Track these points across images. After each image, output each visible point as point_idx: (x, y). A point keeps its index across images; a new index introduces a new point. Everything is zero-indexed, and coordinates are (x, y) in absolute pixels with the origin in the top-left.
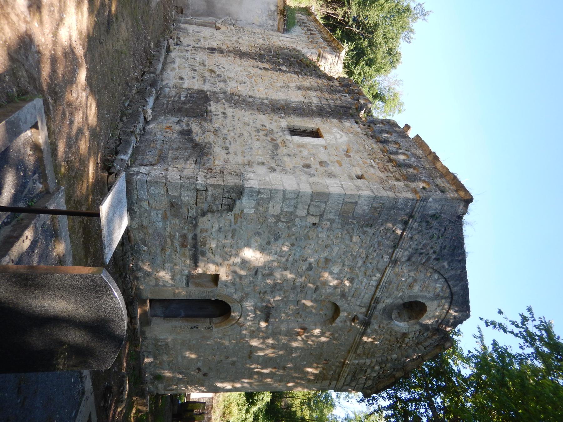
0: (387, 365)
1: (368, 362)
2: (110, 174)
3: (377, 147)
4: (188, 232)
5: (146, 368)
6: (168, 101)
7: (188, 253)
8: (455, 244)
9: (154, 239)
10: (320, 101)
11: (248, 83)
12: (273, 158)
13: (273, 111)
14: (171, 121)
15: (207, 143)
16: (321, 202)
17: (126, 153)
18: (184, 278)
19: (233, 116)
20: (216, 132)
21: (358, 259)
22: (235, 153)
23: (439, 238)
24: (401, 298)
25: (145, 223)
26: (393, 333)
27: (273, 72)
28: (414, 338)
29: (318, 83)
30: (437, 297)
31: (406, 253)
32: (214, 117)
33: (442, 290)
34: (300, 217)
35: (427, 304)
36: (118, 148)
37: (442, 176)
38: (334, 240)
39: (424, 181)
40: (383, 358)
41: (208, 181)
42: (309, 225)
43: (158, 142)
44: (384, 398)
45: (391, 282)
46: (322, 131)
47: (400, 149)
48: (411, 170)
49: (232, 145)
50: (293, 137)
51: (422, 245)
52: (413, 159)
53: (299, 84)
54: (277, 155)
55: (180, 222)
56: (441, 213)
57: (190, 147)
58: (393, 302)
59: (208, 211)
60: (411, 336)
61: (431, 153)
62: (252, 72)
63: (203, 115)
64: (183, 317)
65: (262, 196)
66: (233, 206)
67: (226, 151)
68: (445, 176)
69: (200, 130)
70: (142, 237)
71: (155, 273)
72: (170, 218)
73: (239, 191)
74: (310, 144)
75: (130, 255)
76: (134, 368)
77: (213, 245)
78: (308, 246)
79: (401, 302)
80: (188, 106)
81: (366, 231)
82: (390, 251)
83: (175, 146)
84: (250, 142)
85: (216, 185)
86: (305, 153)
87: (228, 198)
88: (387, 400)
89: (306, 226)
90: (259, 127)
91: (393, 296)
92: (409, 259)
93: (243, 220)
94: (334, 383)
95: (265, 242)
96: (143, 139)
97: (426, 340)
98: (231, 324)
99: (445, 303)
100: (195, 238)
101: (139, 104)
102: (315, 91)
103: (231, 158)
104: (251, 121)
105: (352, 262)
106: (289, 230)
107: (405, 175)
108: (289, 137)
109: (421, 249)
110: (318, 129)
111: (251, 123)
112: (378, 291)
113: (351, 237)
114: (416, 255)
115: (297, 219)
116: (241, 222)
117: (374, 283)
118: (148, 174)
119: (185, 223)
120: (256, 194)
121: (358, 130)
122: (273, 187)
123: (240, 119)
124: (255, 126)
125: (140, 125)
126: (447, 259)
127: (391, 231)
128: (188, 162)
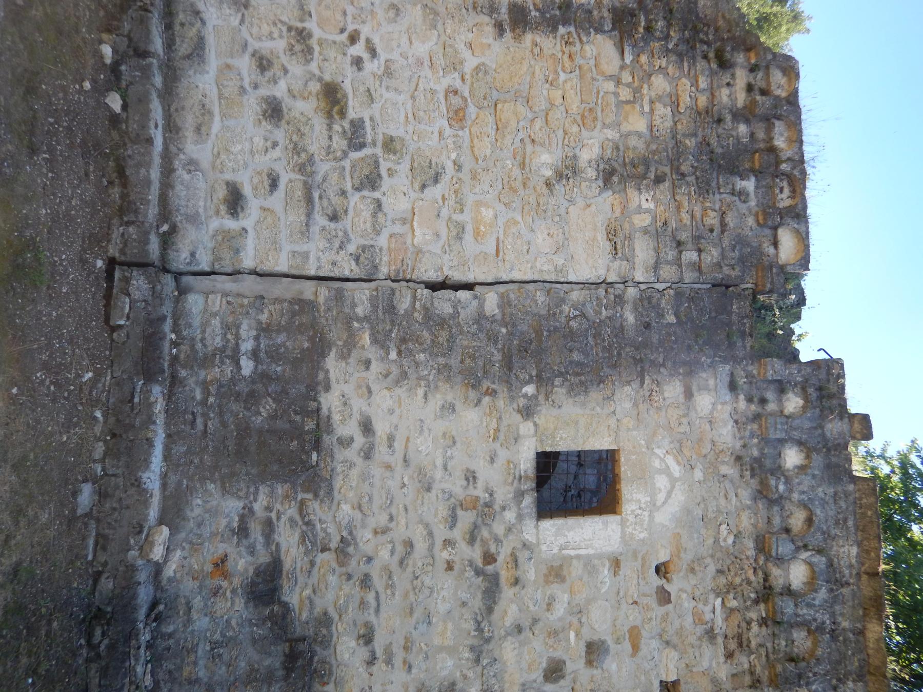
6: (205, 385)
10: (656, 267)
11: (449, 166)
12: (477, 661)
22: (389, 662)
29: (675, 104)
32: (341, 454)
43: (200, 652)
46: (625, 469)
47: (805, 547)
49: (383, 614)
52: (823, 594)
54: (488, 641)
57: (278, 665)
63: (307, 466)
67: (363, 653)
68: (870, 673)
74: (578, 557)
90: (457, 487)
102: (659, 180)
104: (439, 462)
107: (776, 675)
110: (618, 450)
111: (439, 474)
121: (726, 435)
123: (411, 455)
124: (447, 486)
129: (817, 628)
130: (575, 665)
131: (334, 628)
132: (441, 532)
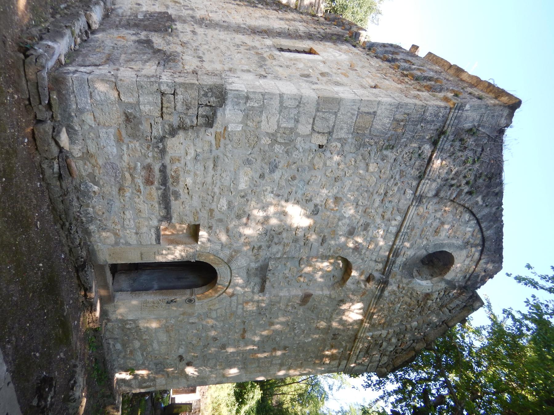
0: (406, 335)
1: (384, 333)
2: (26, 56)
3: (385, 65)
4: (154, 160)
5: (114, 360)
7: (155, 194)
8: (493, 171)
9: (107, 173)
11: (221, 13)
13: (255, 33)
14: (124, 33)
15: (173, 52)
16: (330, 113)
17: (54, 41)
18: (153, 231)
19: (205, 34)
20: (183, 44)
21: (375, 196)
23: (474, 162)
24: (425, 248)
25: (92, 149)
26: (414, 294)
27: (248, 7)
28: (438, 300)
30: (467, 244)
31: (434, 186)
32: (181, 35)
33: (473, 235)
34: (303, 136)
35: (454, 254)
36: (44, 36)
37: (472, 86)
38: (346, 169)
39: (452, 91)
40: (401, 327)
41: (177, 80)
42: (315, 147)
43: (107, 48)
44: (392, 381)
45: (414, 227)
47: (413, 65)
48: (433, 83)
50: (283, 53)
51: (453, 172)
52: (431, 73)
53: (280, 17)
54: (266, 65)
55: (141, 145)
56: (479, 126)
58: (415, 254)
59: (179, 128)
60: (435, 296)
61: (451, 66)
62: (224, 6)
64: (156, 290)
65: (252, 104)
66: (213, 118)
68: (476, 87)
69: (163, 42)
70: (90, 170)
71: (113, 225)
72: (127, 140)
73: (219, 95)
75: (75, 200)
76: (96, 359)
77: (189, 181)
78: (313, 179)
79: (425, 253)
80: (146, 23)
81: (386, 156)
82: (414, 183)
83: (130, 51)
84: (229, 53)
85: (188, 84)
86: (301, 65)
87: (206, 105)
88: (395, 383)
89: (310, 150)
91: (416, 246)
92: (436, 195)
93: (228, 141)
94: (344, 362)
95: (258, 175)
96: (85, 44)
97: (451, 301)
98: (217, 295)
99: (475, 252)
100: (163, 169)
101: (80, 9)
103: (205, 65)
105: (368, 201)
106: (288, 155)
108: (278, 53)
109: (453, 179)
110: (311, 49)
112: (398, 241)
113: (367, 165)
114: (445, 188)
115: (299, 139)
116: (225, 145)
117: (394, 230)
118: (90, 73)
119: (148, 148)
120: (245, 100)
122: (266, 91)
125: (80, 24)
126: (482, 193)
127: (417, 155)
128: (147, 64)
129: (437, 79)
130: (315, 75)
131: (181, 55)
132: (233, 49)
